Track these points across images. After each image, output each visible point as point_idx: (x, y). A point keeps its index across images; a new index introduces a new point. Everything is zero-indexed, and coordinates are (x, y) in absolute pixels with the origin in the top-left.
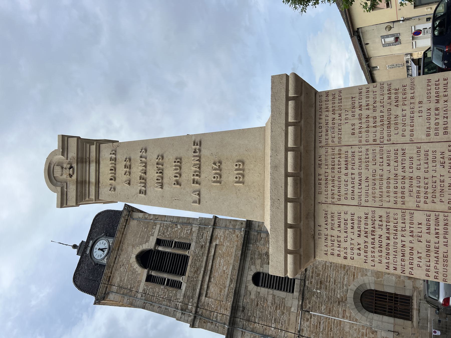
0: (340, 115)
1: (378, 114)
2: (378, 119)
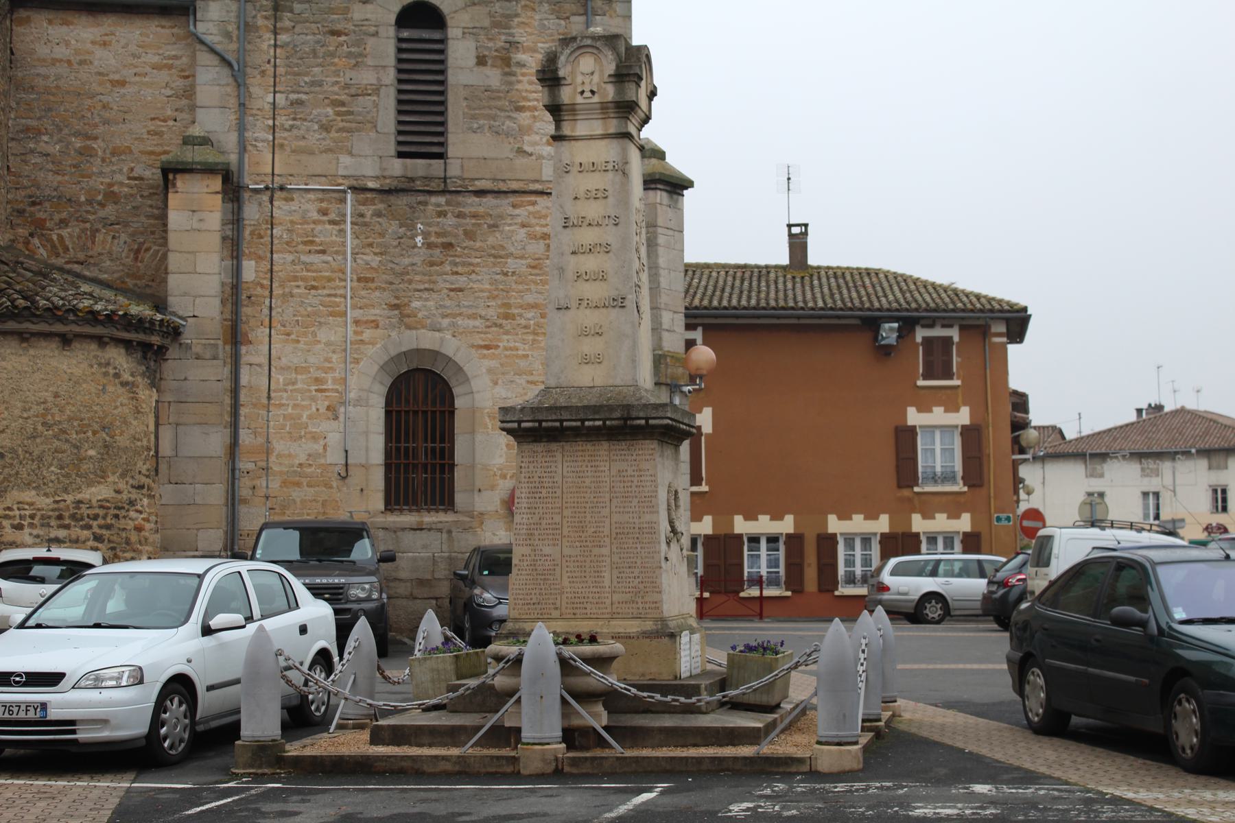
1: (634, 489)
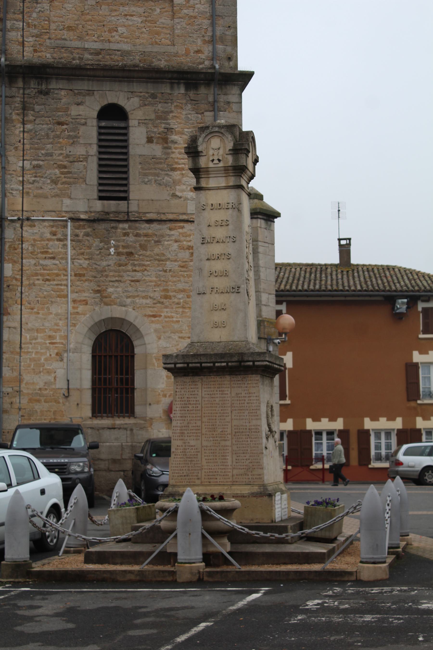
0: (246, 387)
1: (246, 405)
2: (243, 405)
